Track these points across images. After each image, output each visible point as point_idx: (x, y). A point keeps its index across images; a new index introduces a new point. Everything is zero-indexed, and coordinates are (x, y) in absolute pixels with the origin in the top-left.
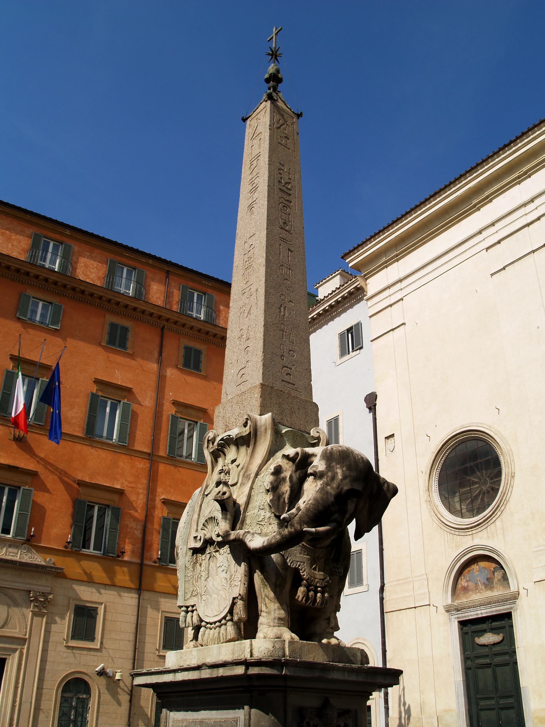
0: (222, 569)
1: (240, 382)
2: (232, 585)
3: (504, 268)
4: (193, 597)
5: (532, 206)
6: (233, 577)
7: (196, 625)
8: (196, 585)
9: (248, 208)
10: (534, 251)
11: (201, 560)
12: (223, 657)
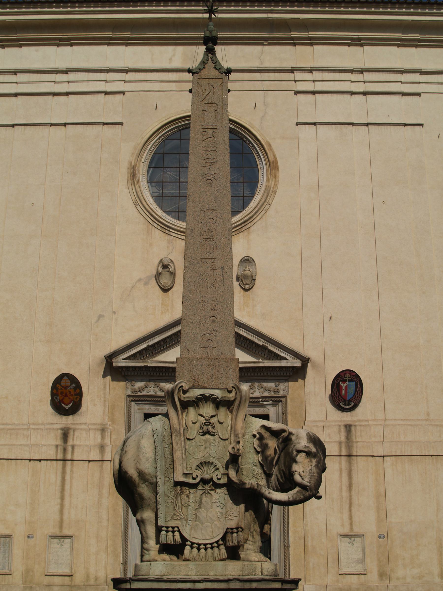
0: (218, 504)
1: (206, 344)
2: (227, 518)
3: (13, 126)
4: (173, 520)
5: (64, 77)
6: (228, 513)
7: (179, 543)
8: (178, 511)
9: (204, 177)
10: (51, 125)
11: (188, 491)
12: (230, 572)
